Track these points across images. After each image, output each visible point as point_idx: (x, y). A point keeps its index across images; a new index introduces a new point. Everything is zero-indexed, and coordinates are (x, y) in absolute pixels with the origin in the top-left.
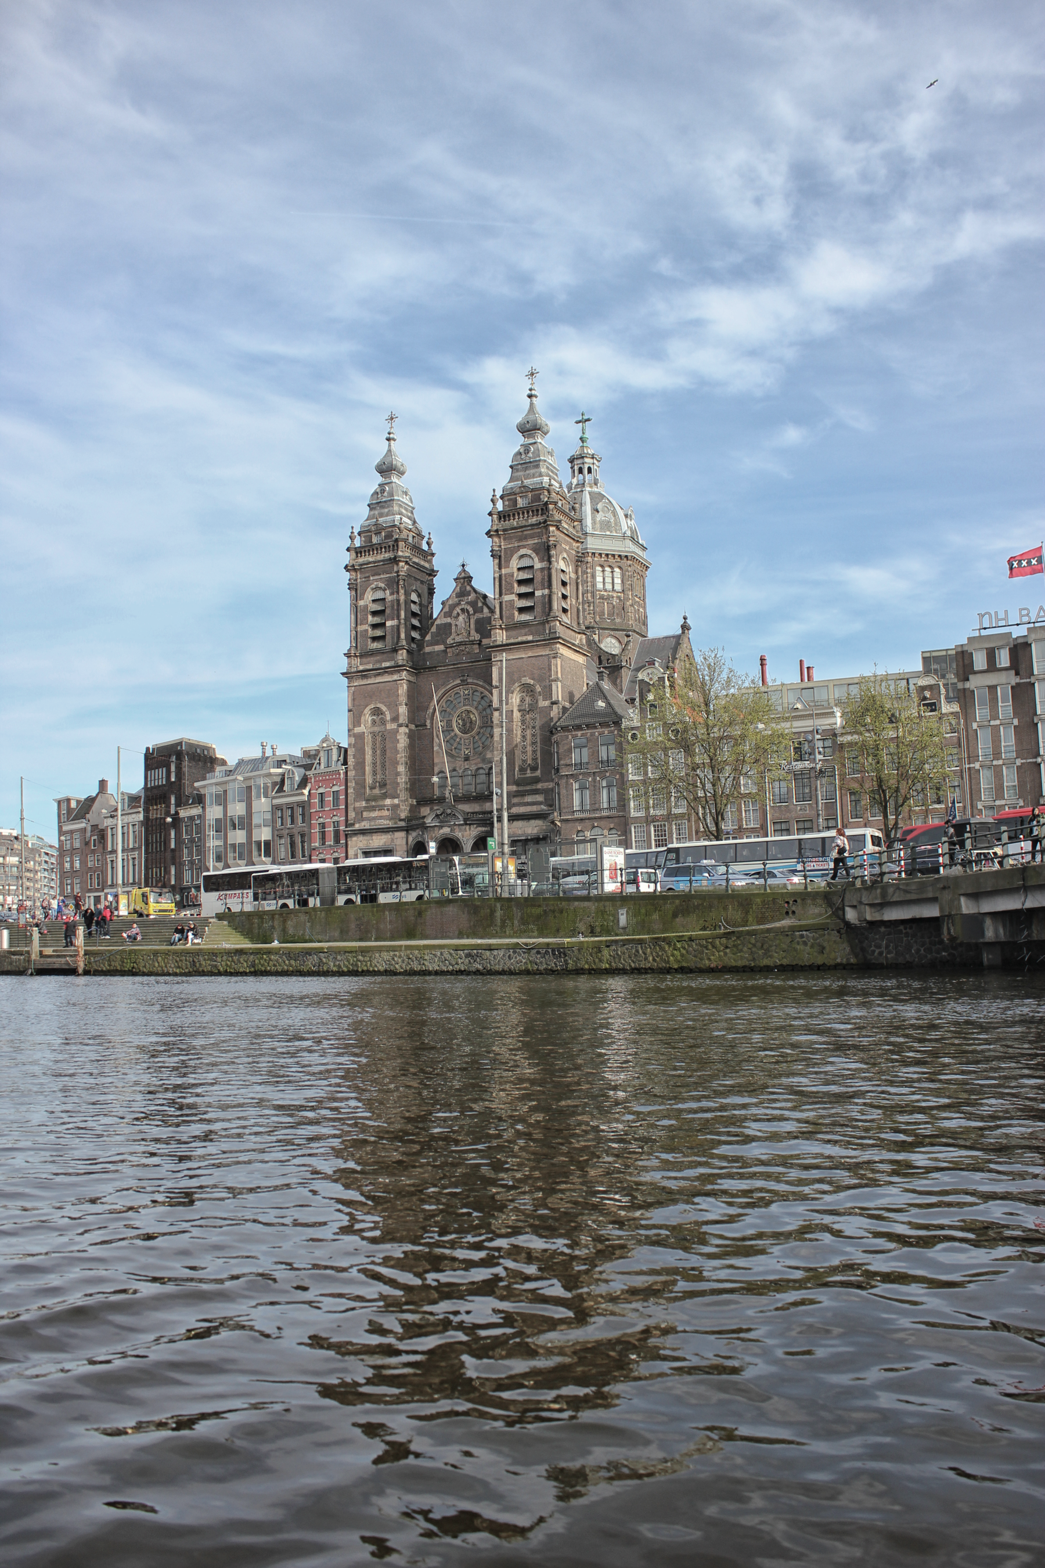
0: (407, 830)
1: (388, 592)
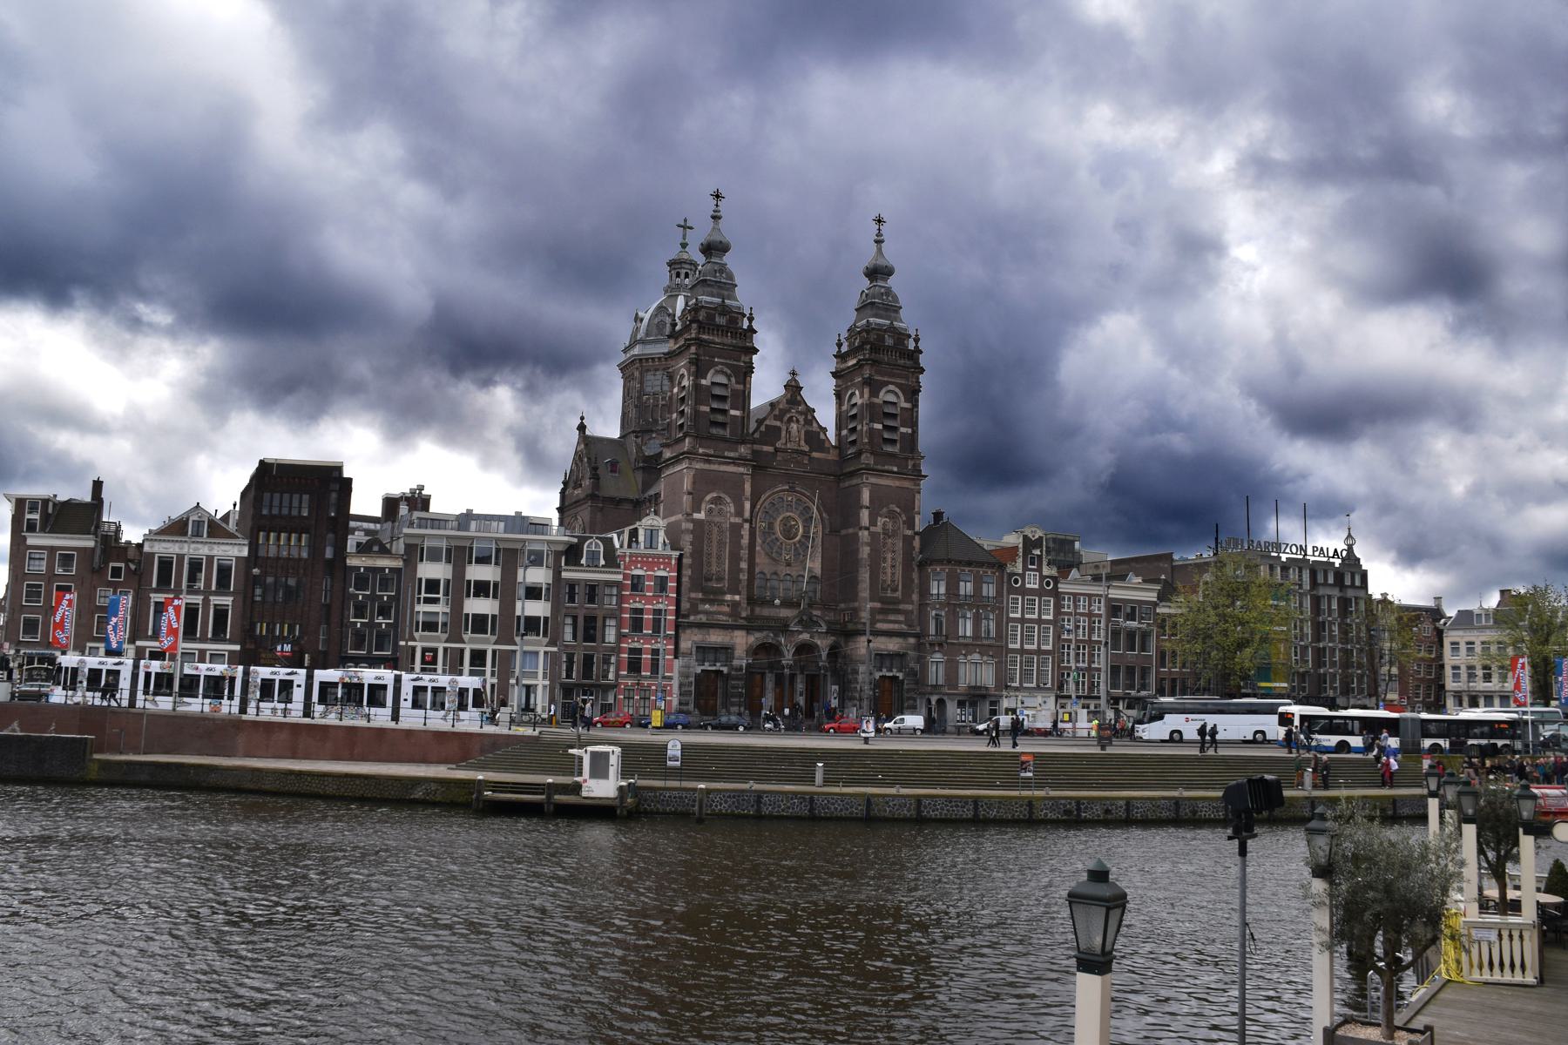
0: (749, 629)
1: (733, 379)
